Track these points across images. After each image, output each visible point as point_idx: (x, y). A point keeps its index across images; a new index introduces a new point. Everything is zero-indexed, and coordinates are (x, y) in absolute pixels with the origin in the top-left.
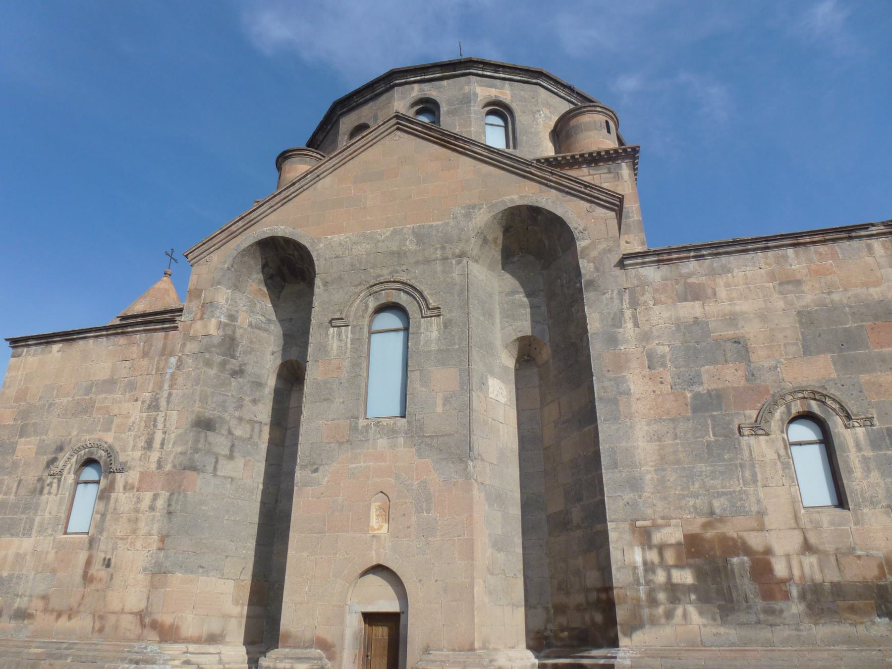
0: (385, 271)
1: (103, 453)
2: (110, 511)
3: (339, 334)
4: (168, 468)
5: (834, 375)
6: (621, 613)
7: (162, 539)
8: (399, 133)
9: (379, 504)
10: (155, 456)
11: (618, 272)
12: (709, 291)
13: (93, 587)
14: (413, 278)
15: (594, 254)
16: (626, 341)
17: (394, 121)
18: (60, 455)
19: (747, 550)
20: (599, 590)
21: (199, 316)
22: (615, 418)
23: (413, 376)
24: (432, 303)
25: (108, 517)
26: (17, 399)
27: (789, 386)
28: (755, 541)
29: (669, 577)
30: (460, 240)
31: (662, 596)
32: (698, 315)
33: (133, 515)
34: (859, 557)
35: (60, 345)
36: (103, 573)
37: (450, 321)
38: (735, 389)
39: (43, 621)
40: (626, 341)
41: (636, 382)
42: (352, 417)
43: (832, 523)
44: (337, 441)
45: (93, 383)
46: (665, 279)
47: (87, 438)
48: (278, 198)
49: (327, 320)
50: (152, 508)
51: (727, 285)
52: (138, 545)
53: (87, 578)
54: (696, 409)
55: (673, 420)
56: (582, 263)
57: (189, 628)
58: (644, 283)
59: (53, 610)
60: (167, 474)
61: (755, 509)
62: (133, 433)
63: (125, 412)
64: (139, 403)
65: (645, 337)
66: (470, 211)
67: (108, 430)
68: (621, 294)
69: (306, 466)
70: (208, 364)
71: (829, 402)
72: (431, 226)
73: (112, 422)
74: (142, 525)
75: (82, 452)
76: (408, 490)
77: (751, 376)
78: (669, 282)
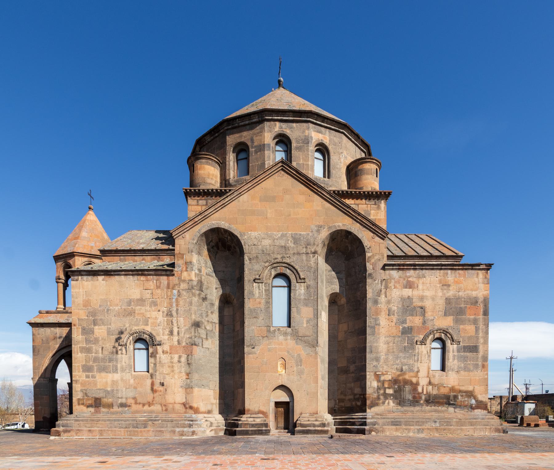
0: (279, 257)
1: (147, 336)
2: (158, 362)
3: (259, 287)
4: (184, 344)
5: (452, 325)
6: (368, 402)
7: (188, 374)
8: (283, 172)
10: (175, 338)
11: (382, 271)
12: (416, 285)
13: (156, 394)
14: (293, 262)
15: (373, 261)
16: (381, 303)
17: (280, 164)
18: (122, 336)
19: (411, 383)
20: (361, 395)
21: (184, 269)
22: (373, 334)
23: (293, 310)
24: (302, 277)
25: (158, 365)
26: (85, 306)
27: (436, 328)
28: (414, 380)
29: (385, 391)
30: (314, 244)
31: (382, 397)
32: (410, 295)
33: (170, 364)
34: (444, 387)
35: (103, 277)
36: (161, 388)
37: (310, 285)
38: (418, 327)
39: (134, 407)
40: (381, 303)
41: (383, 321)
42: (268, 326)
43: (439, 376)
45: (131, 300)
46: (400, 277)
47: (135, 328)
48: (219, 204)
49: (252, 279)
50: (179, 362)
51: (423, 283)
52: (176, 377)
53: (152, 389)
54: (403, 333)
55: (394, 337)
56: (368, 264)
57: (202, 409)
58: (391, 278)
59: (140, 403)
60: (184, 347)
61: (416, 370)
62: (161, 327)
63: (154, 317)
64: (161, 313)
65: (389, 302)
66: (319, 228)
67: (147, 325)
68: (381, 282)
70: (194, 295)
71: (448, 335)
72: (300, 235)
73: (148, 321)
74: (176, 368)
75: (135, 335)
77: (424, 322)
78: (401, 279)
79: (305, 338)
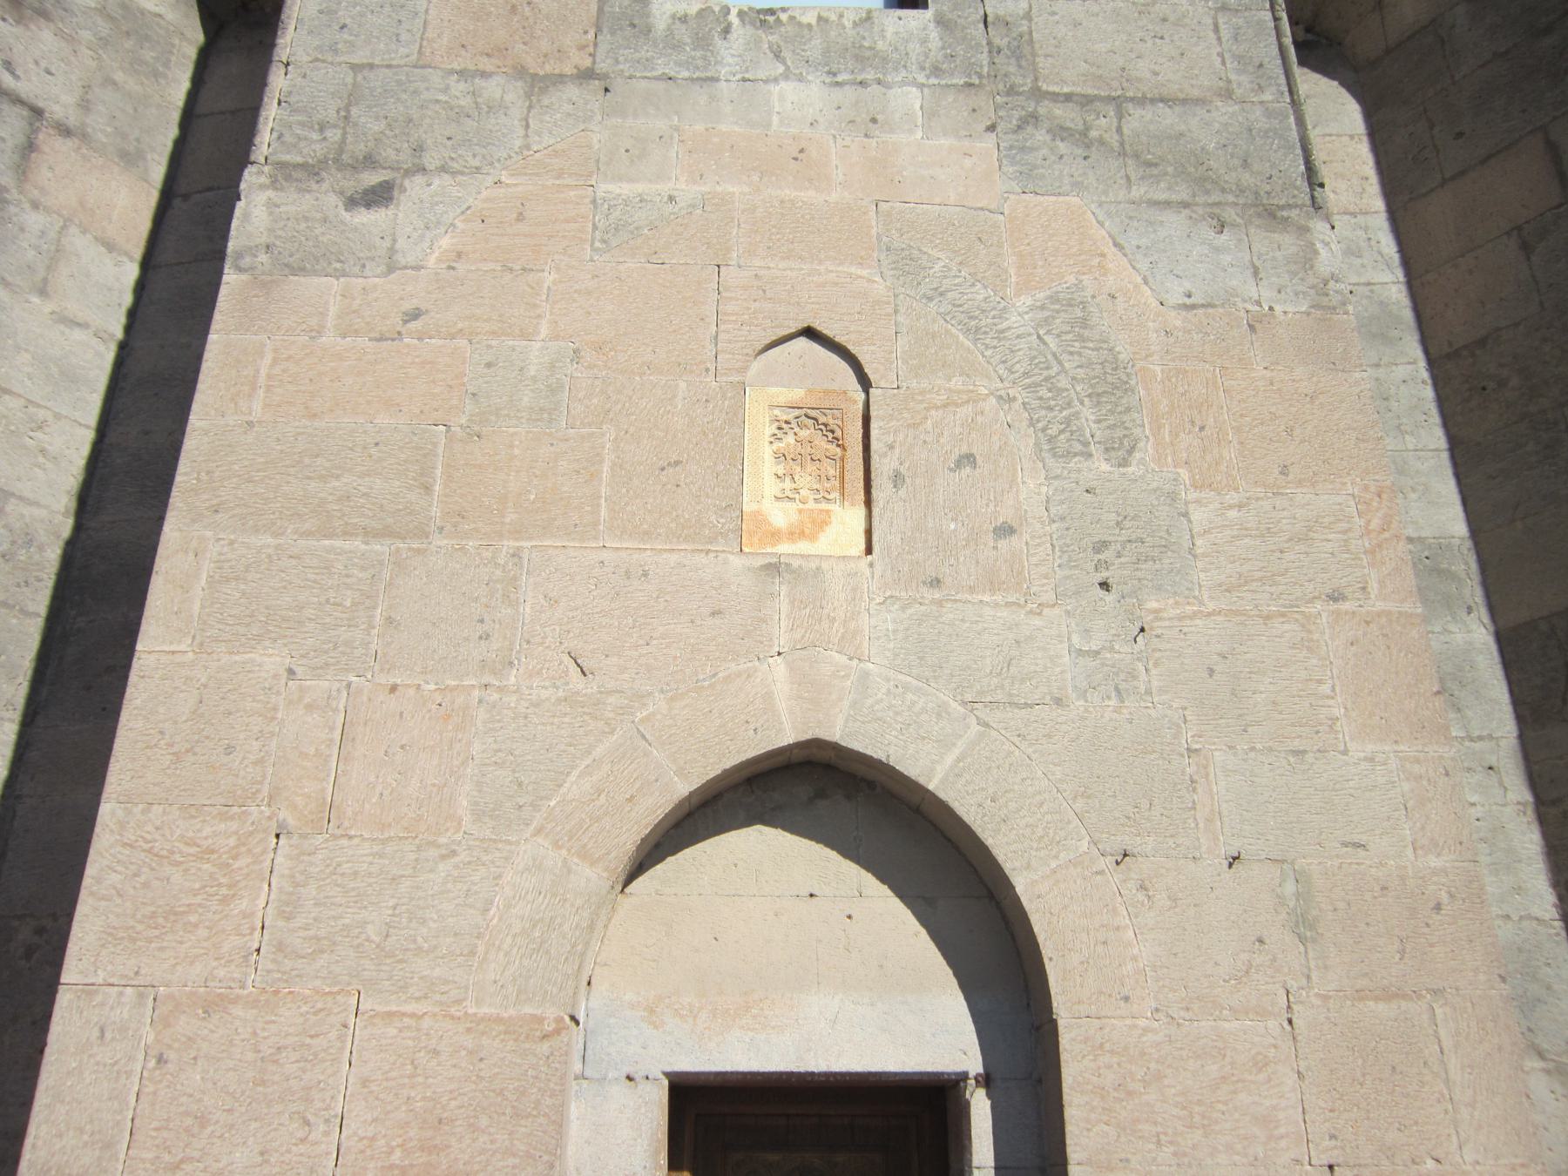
9: (796, 394)
44: (520, 72)
69: (313, 171)
76: (975, 333)
79: (1137, 119)
